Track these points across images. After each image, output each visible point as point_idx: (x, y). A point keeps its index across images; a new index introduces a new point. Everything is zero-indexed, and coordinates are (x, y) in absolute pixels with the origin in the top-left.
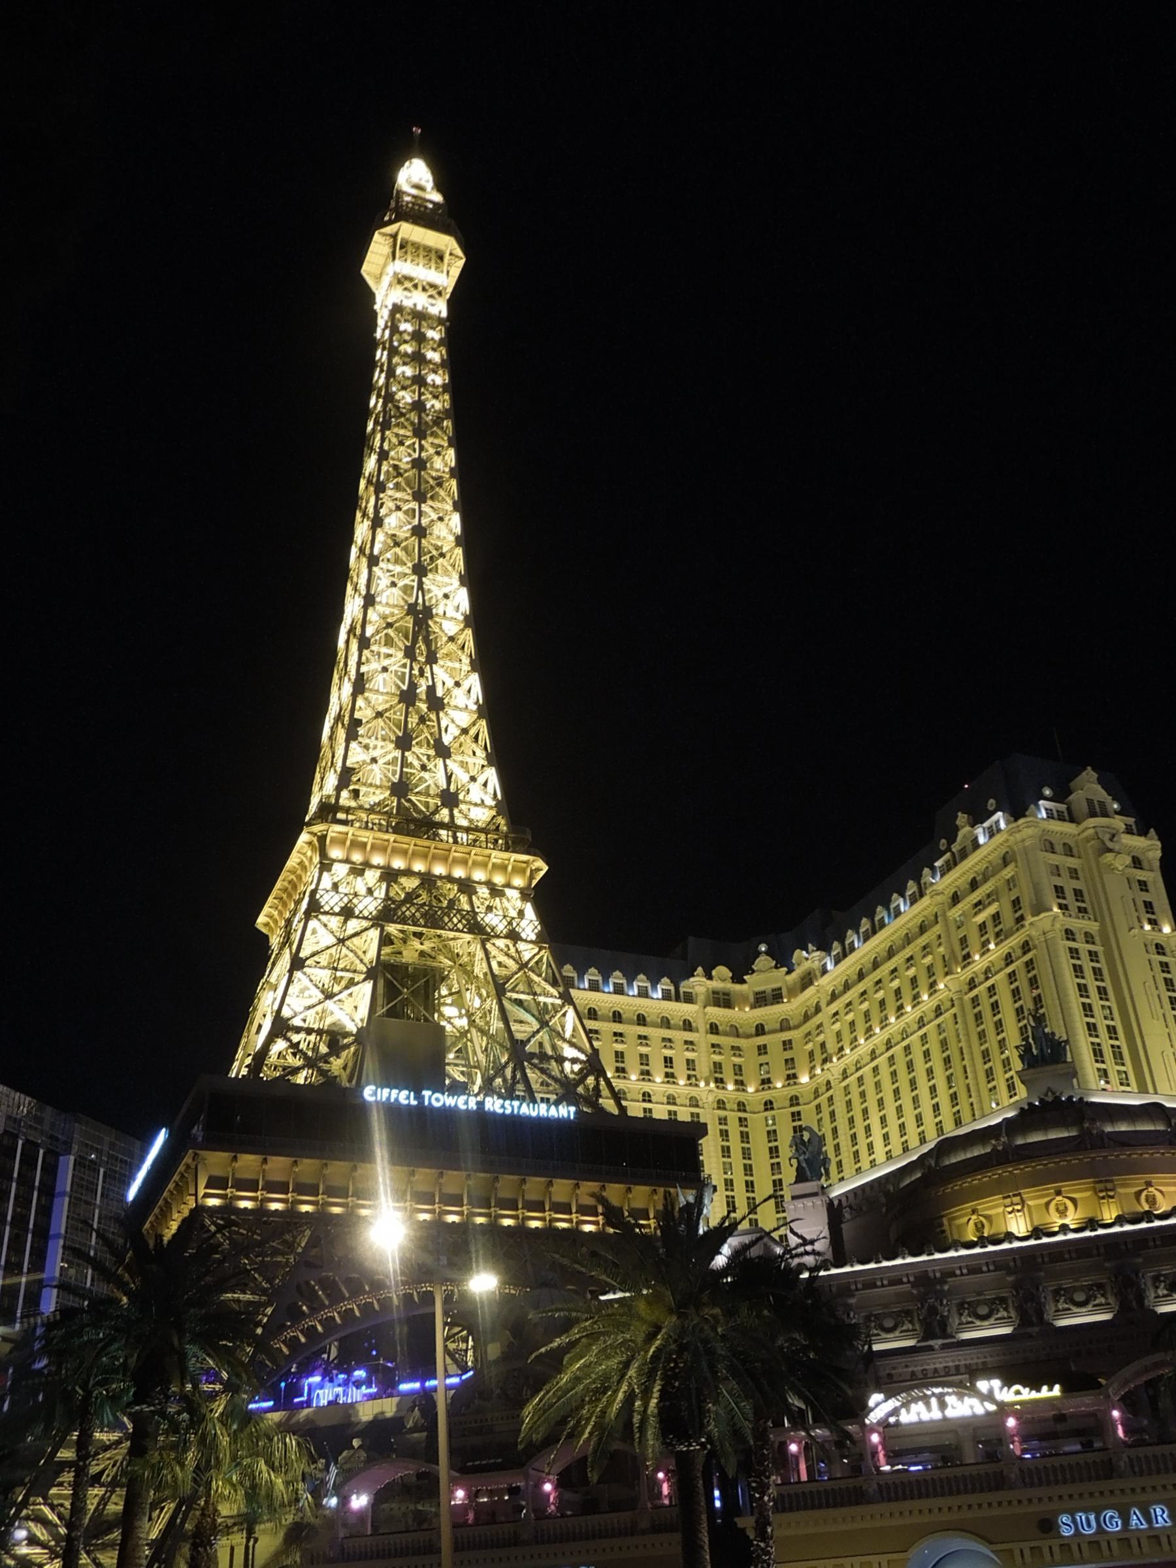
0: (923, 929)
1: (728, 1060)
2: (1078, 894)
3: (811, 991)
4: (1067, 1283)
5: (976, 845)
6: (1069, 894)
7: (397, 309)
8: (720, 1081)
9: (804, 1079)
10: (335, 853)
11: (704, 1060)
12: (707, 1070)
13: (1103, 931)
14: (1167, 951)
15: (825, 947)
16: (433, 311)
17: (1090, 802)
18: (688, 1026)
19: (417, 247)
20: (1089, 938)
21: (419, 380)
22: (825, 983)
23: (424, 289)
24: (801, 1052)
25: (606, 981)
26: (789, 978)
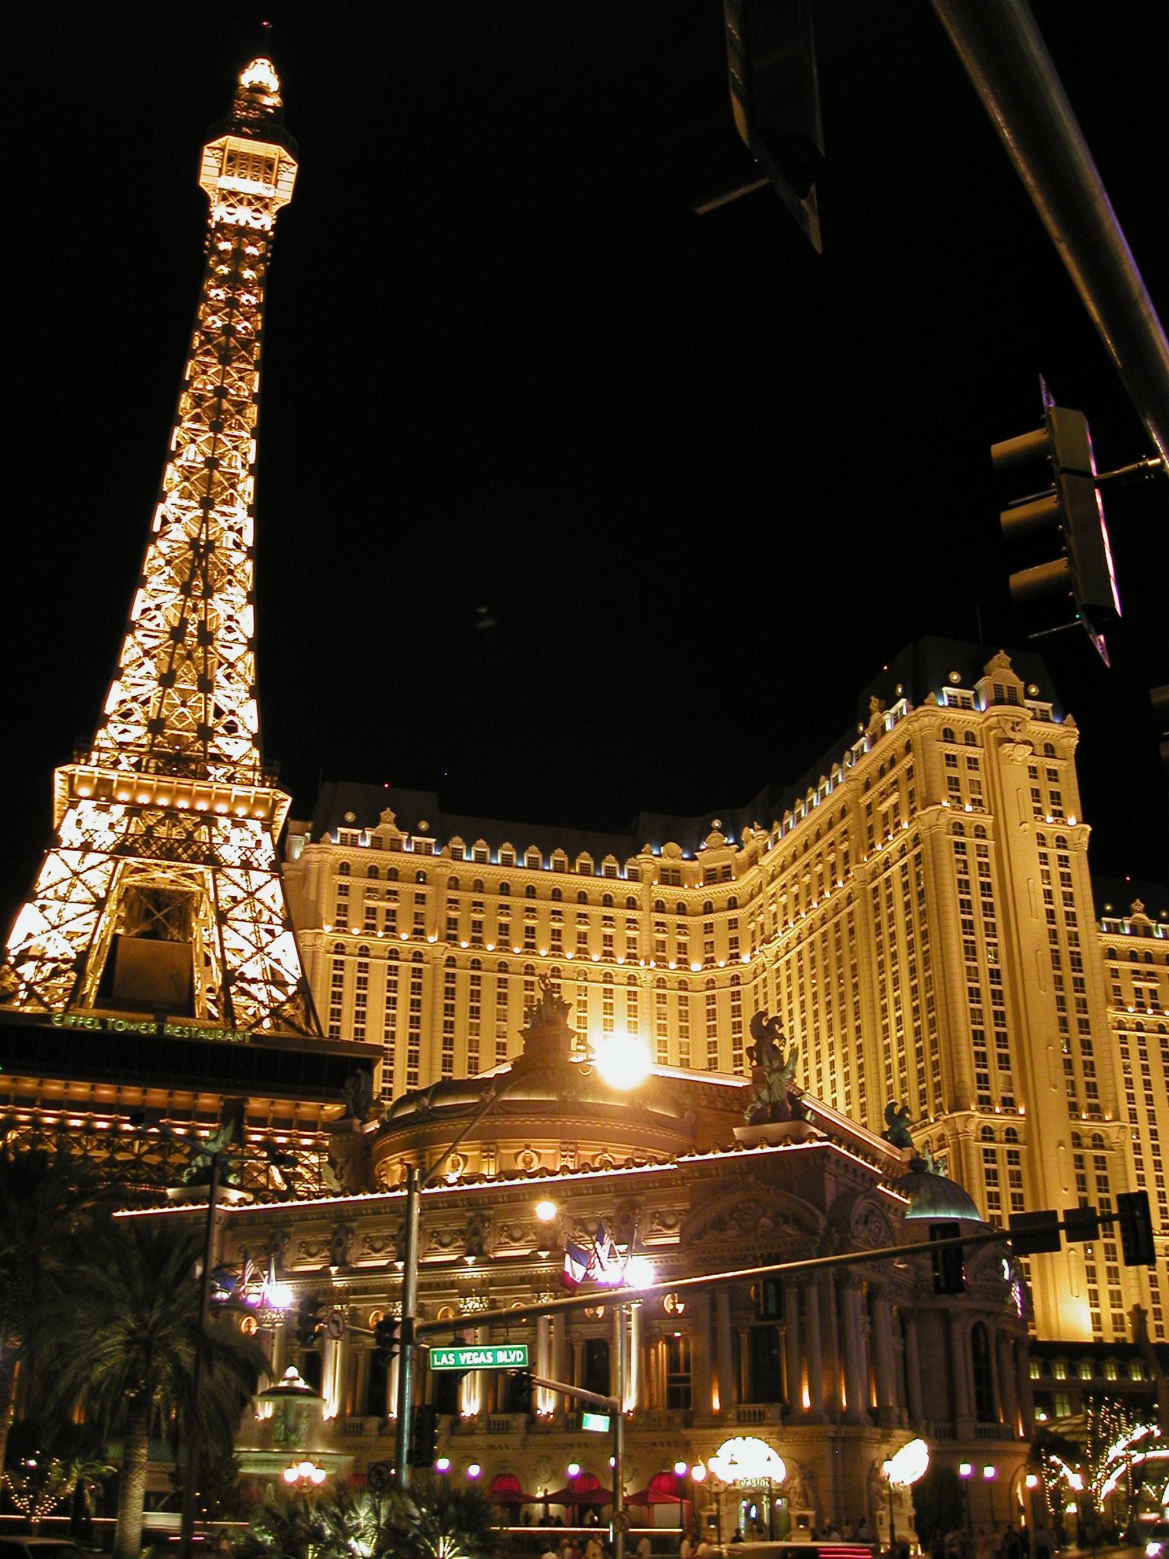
0: (843, 813)
3: (754, 870)
4: (440, 1227)
5: (884, 732)
6: (964, 784)
7: (221, 226)
8: (662, 962)
9: (745, 958)
10: (85, 791)
11: (645, 938)
12: (648, 948)
14: (1069, 844)
16: (256, 225)
17: (998, 688)
18: (631, 904)
19: (246, 157)
20: (980, 832)
21: (232, 303)
22: (768, 862)
23: (250, 204)
25: (546, 859)
26: (738, 855)
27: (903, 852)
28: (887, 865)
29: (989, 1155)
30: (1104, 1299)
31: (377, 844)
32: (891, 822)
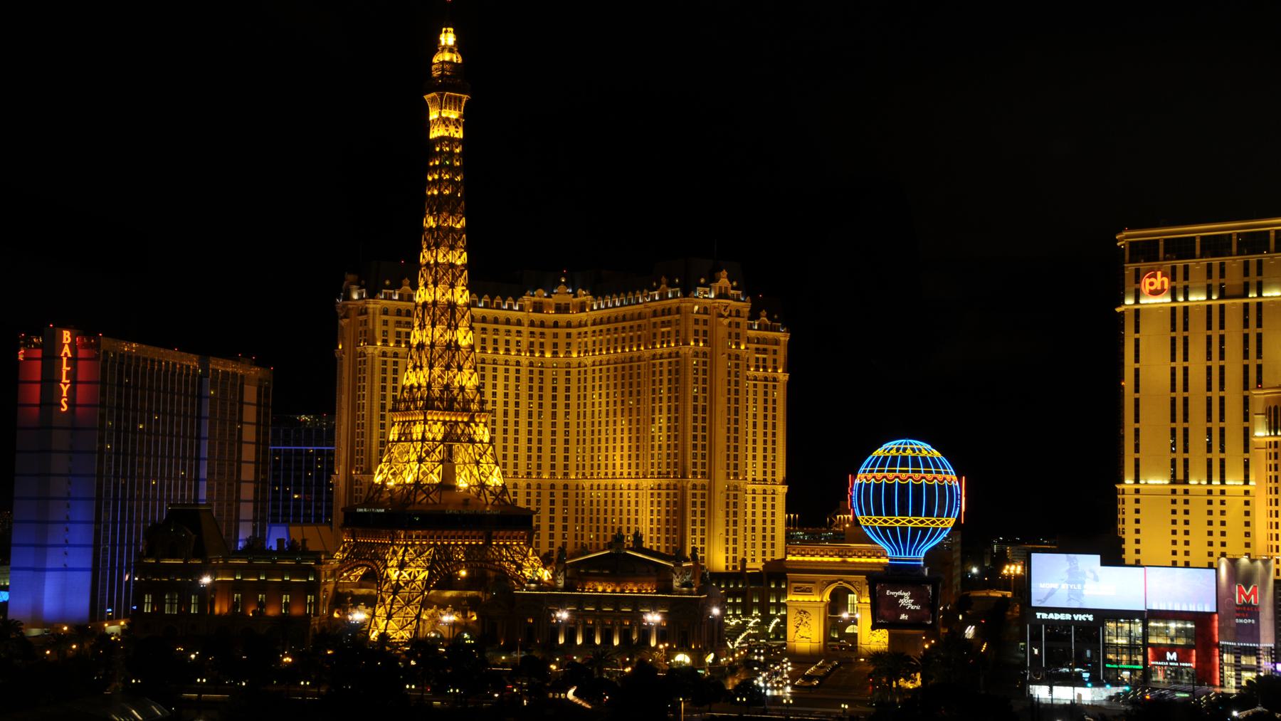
1: (537, 340)
2: (705, 333)
6: (701, 333)
8: (532, 352)
9: (575, 355)
10: (429, 418)
11: (525, 341)
13: (711, 352)
15: (596, 294)
16: (457, 136)
18: (519, 323)
19: (450, 97)
21: (451, 181)
24: (575, 341)
27: (670, 355)
28: (661, 357)
29: (694, 495)
30: (731, 550)
31: (401, 299)
32: (666, 338)
